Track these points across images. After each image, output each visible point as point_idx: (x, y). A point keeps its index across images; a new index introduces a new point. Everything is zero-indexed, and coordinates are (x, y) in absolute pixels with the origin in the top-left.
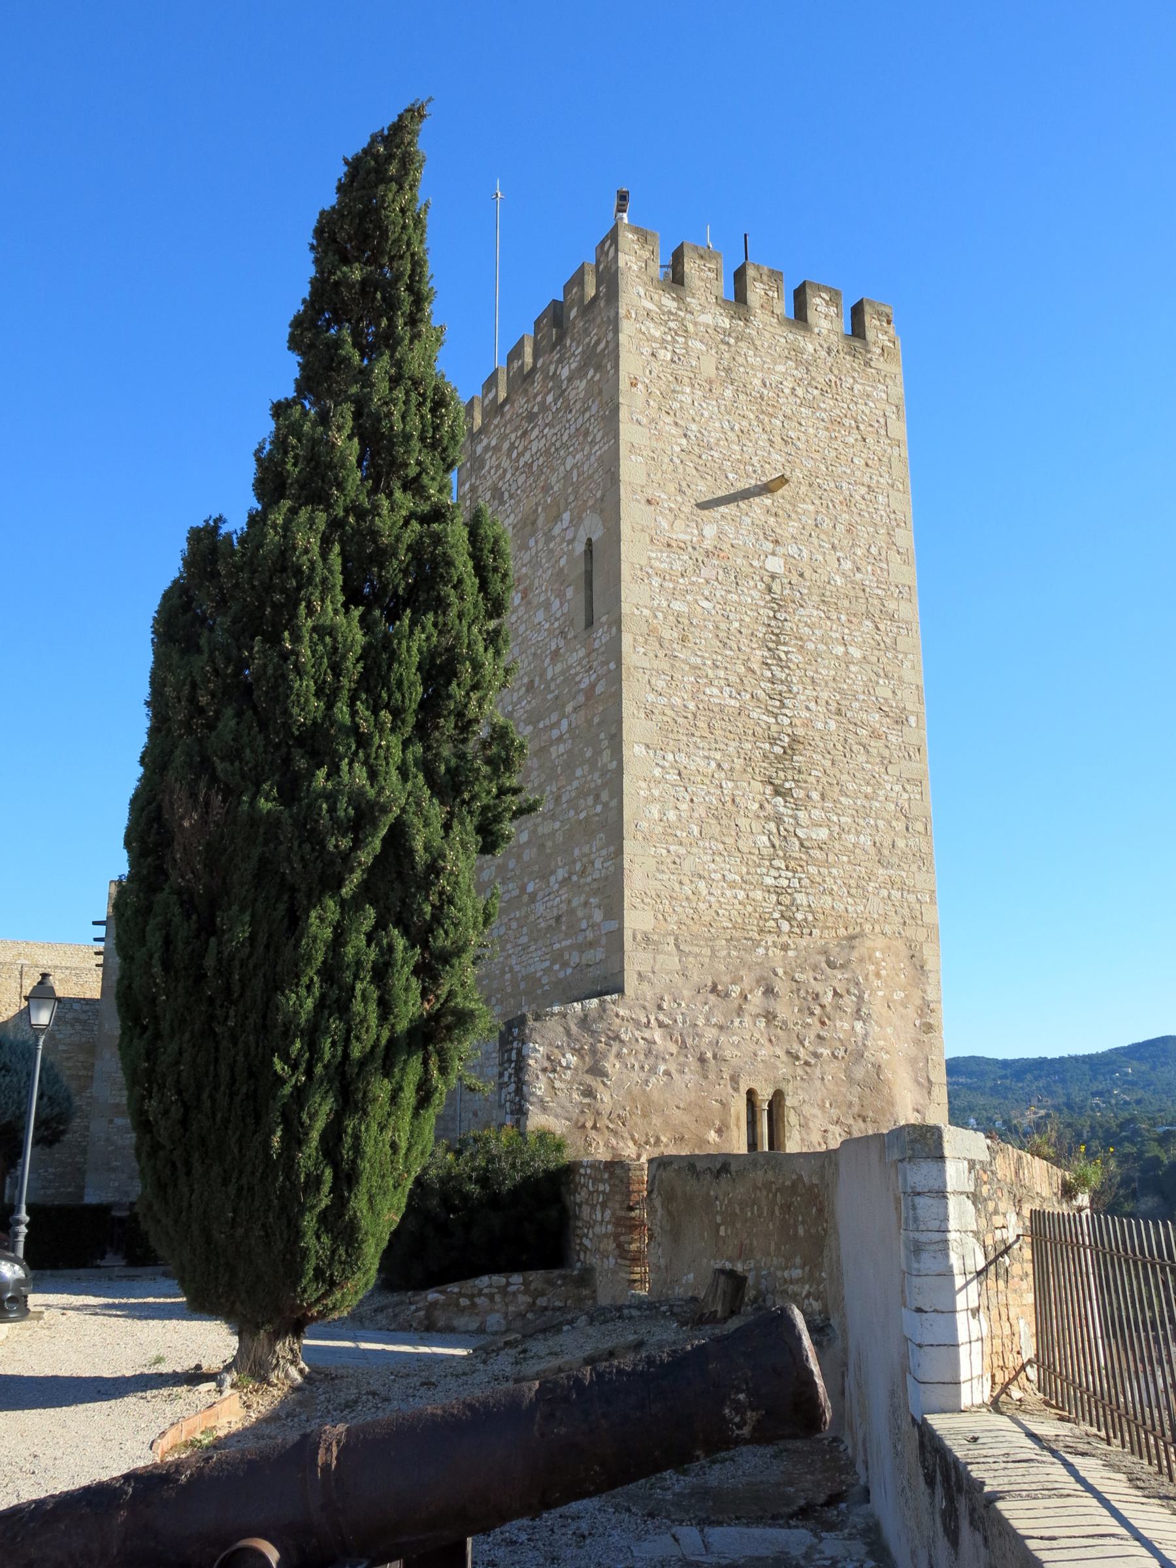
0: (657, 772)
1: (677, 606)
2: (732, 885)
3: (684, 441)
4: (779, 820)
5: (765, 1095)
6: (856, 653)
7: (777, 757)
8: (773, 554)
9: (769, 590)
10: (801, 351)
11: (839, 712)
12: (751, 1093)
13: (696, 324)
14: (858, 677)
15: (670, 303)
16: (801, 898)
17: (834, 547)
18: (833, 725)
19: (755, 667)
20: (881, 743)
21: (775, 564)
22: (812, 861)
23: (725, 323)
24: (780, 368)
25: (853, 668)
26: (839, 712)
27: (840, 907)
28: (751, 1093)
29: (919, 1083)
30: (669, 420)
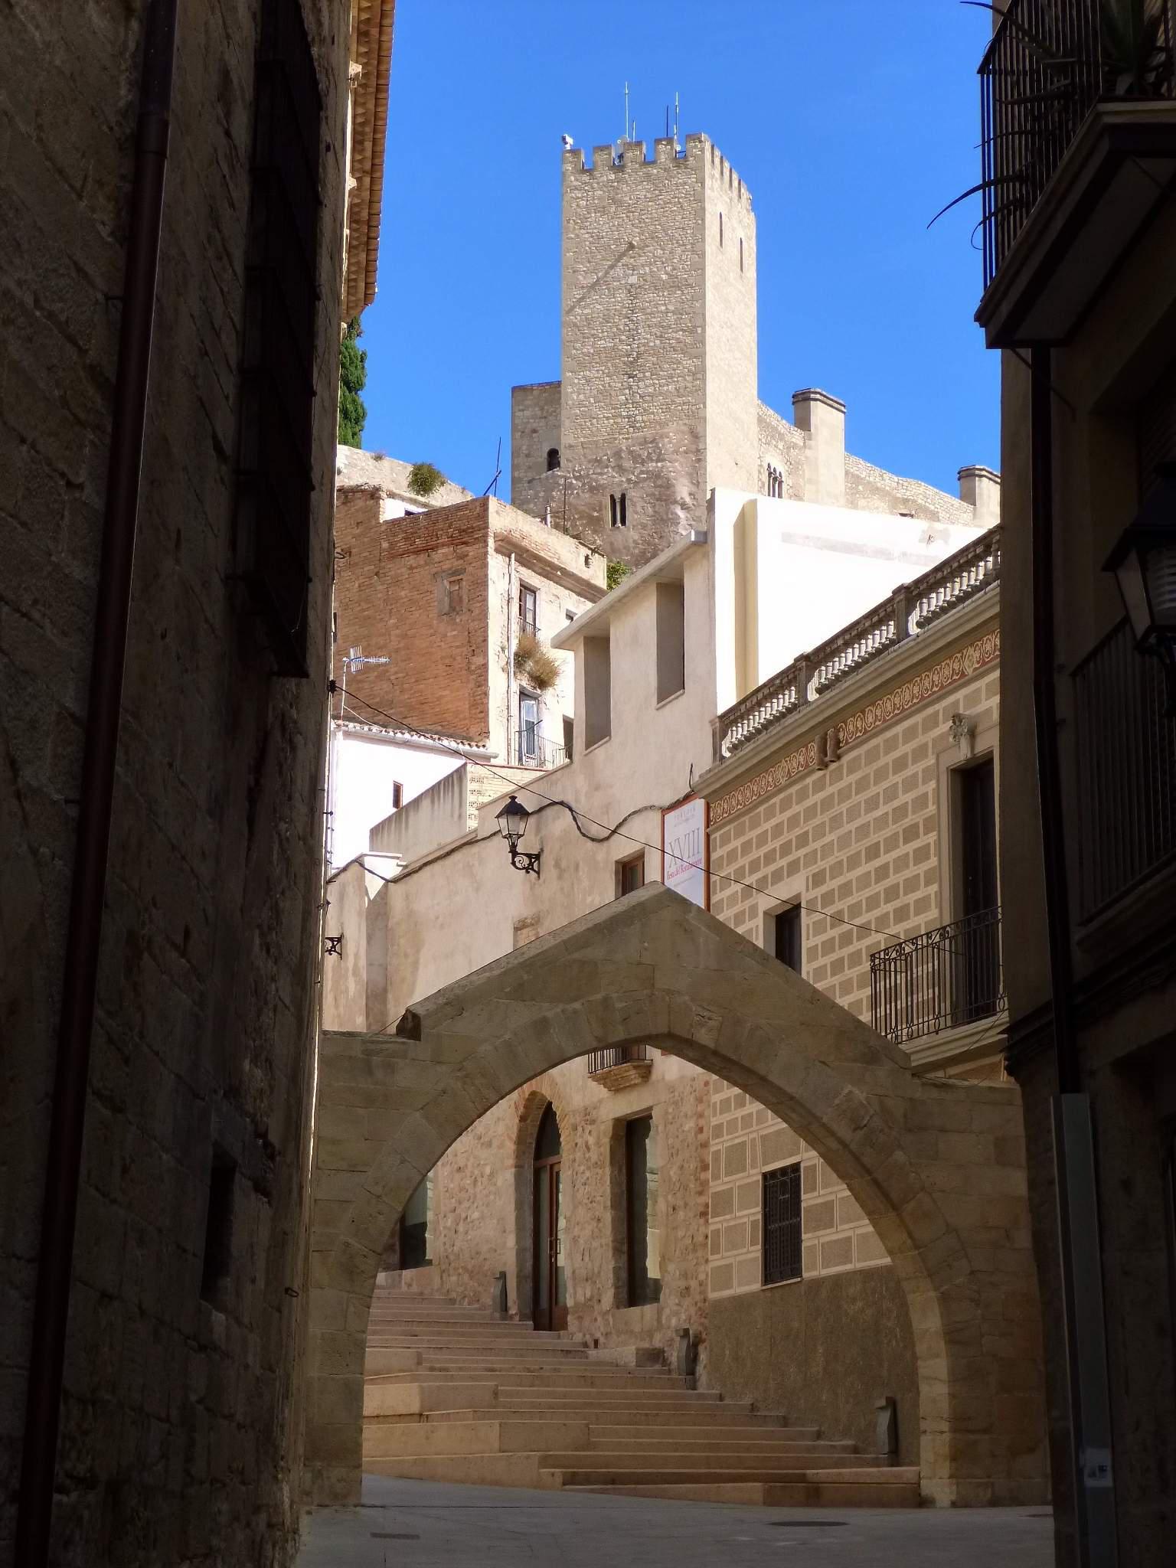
0: (576, 381)
1: (585, 312)
2: (608, 418)
3: (591, 239)
4: (630, 388)
5: (618, 496)
6: (671, 308)
7: (631, 362)
8: (633, 275)
9: (630, 292)
10: (648, 175)
11: (661, 336)
12: (612, 497)
13: (598, 183)
14: (672, 318)
15: (586, 178)
16: (639, 418)
17: (663, 263)
18: (658, 342)
19: (622, 327)
20: (682, 345)
21: (633, 280)
22: (645, 402)
23: (613, 177)
24: (640, 187)
25: (669, 315)
26: (661, 336)
27: (657, 418)
28: (612, 497)
29: (692, 483)
30: (582, 231)
